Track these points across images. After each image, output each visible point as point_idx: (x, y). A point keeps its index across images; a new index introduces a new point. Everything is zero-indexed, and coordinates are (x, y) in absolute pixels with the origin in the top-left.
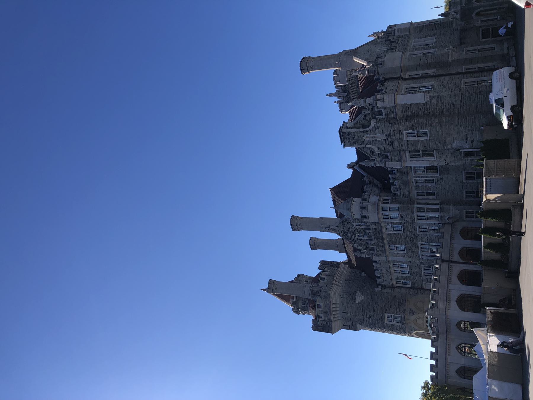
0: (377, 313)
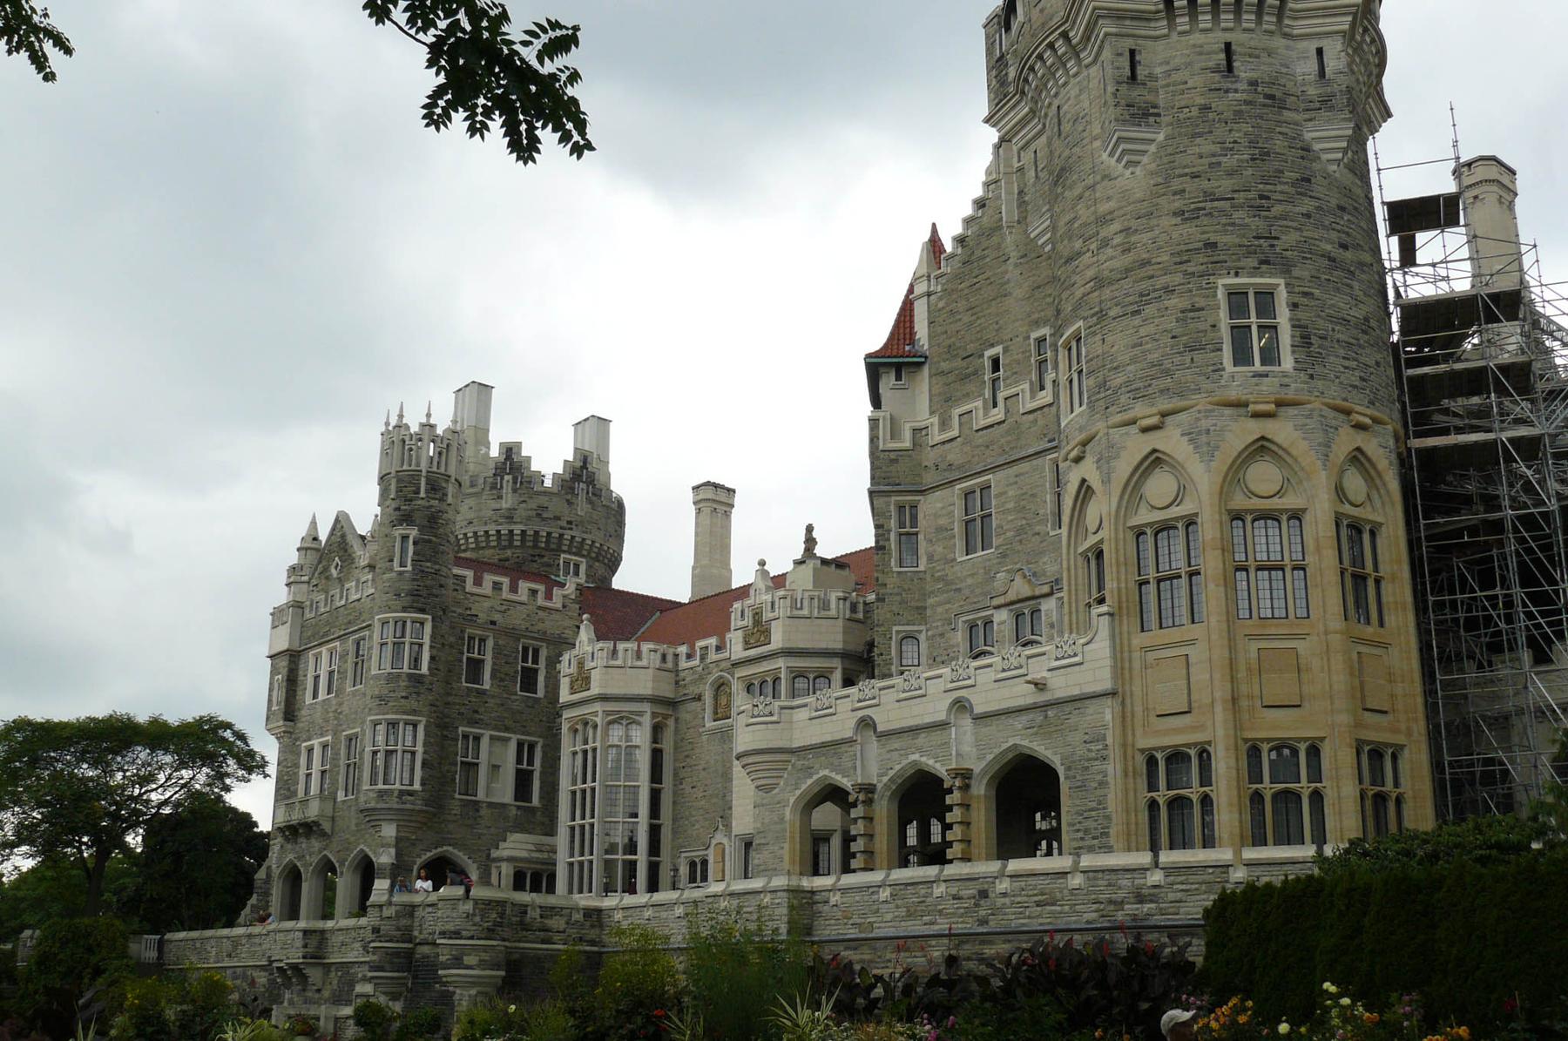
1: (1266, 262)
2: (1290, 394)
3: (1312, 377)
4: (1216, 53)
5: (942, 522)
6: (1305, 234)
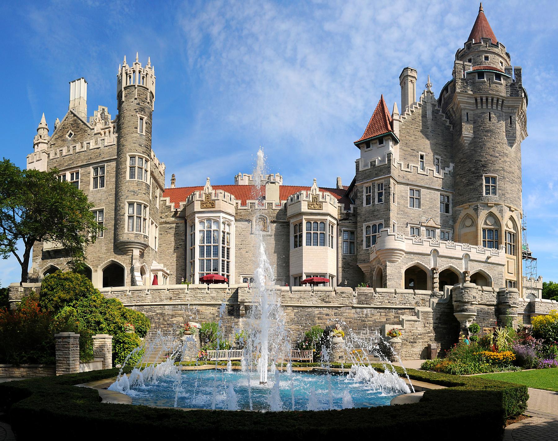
5: (403, 194)
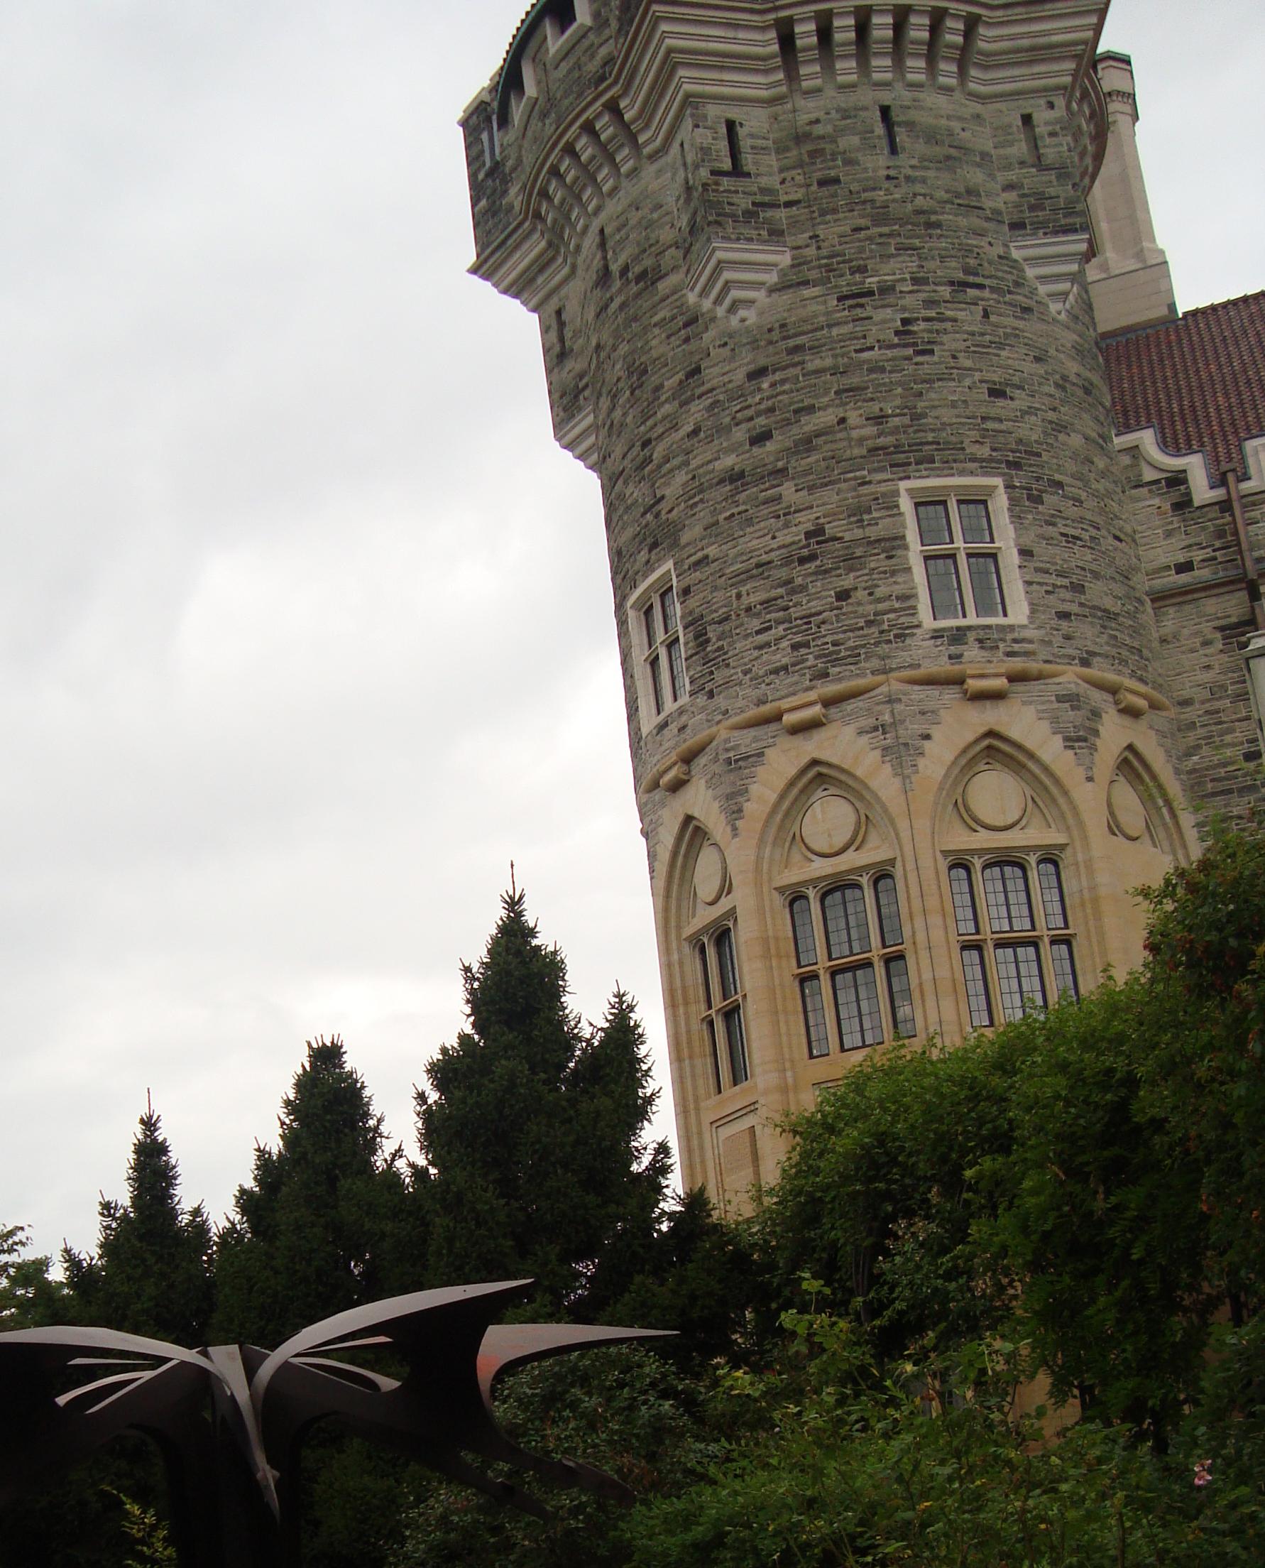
0: (983, 410)
1: (654, 545)
2: (691, 740)
3: (711, 695)
4: (594, 256)
6: (694, 464)
